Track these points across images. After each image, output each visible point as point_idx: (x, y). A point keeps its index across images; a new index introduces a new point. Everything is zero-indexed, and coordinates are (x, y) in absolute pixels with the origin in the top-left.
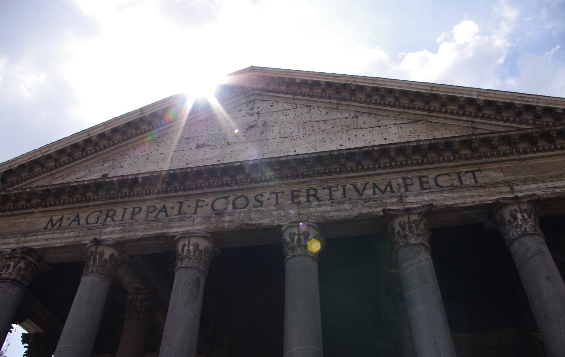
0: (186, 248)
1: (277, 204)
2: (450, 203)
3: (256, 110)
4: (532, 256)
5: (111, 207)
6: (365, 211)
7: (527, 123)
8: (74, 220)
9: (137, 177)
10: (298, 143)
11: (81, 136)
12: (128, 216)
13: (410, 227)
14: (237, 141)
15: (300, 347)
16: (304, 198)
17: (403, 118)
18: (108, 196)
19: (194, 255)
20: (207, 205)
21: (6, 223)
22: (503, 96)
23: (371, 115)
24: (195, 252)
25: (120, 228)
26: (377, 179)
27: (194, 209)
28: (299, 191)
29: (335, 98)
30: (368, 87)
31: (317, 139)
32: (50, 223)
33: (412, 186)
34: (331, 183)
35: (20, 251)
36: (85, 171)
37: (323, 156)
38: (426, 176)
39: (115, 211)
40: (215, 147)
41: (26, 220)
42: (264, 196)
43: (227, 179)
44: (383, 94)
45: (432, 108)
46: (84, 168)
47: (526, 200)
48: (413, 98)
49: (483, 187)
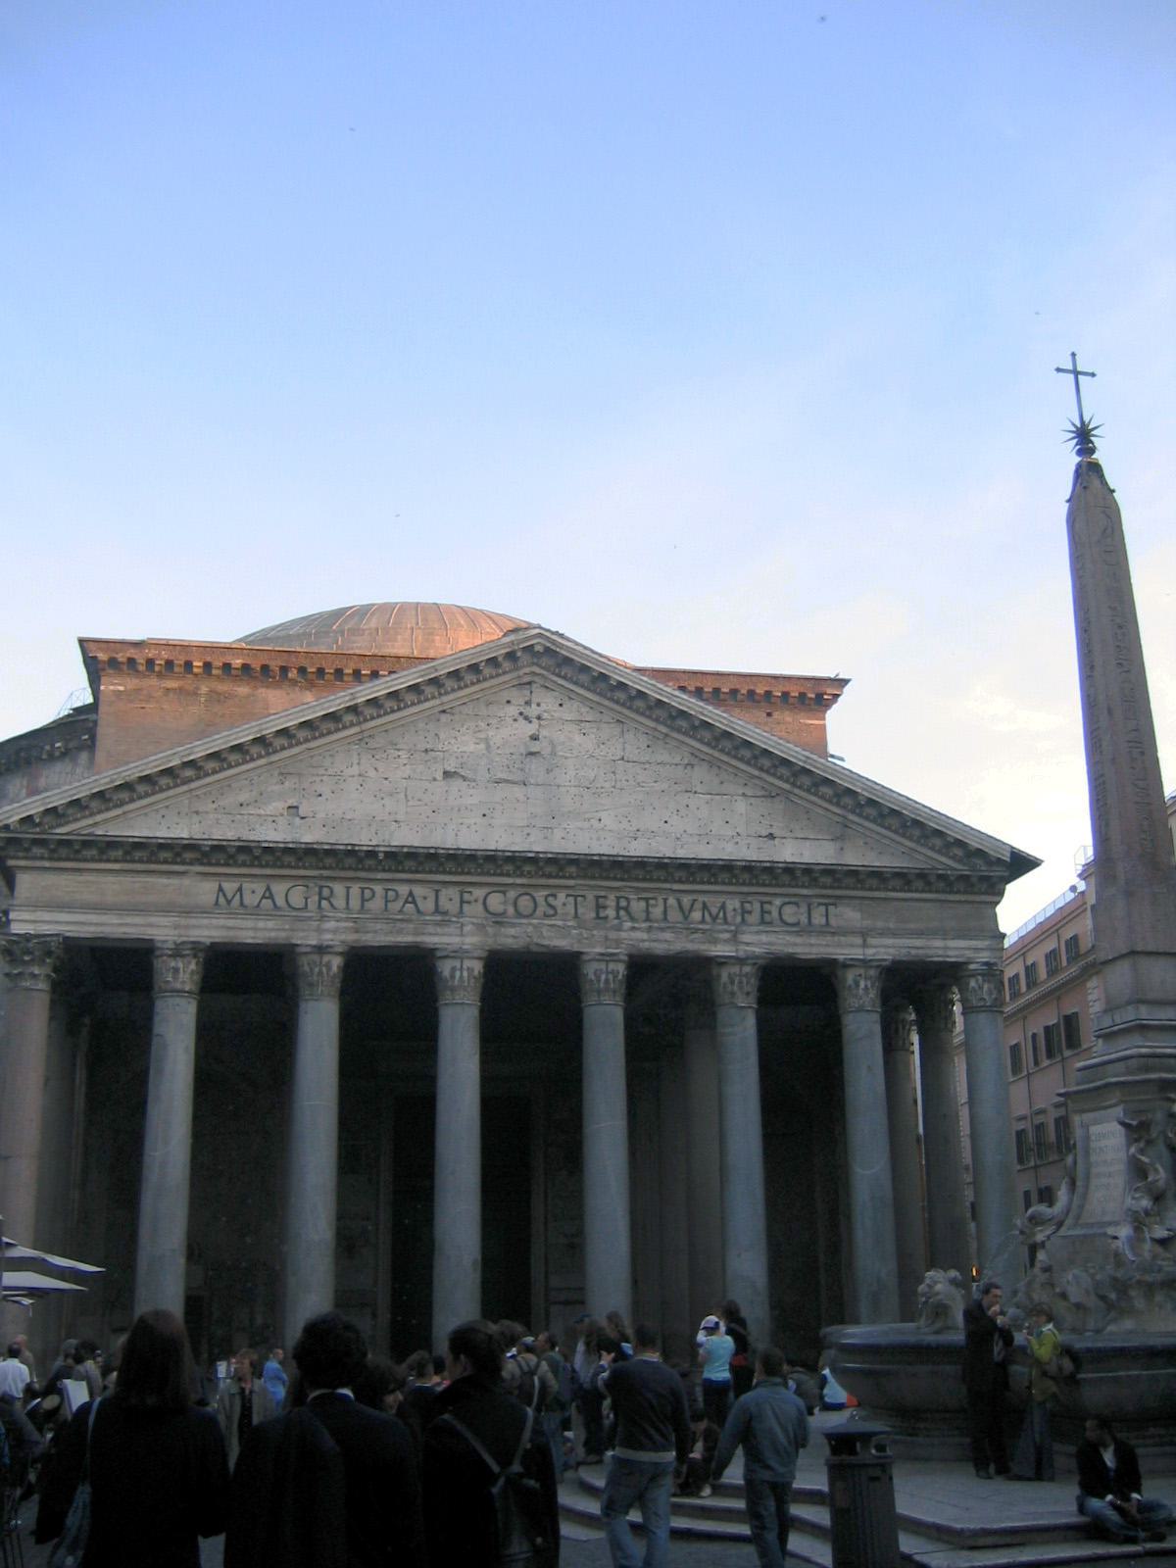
0: (458, 974)
1: (576, 915)
2: (790, 951)
3: (533, 711)
7: (910, 838)
8: (264, 897)
9: (377, 849)
11: (247, 732)
12: (355, 903)
13: (740, 982)
19: (469, 983)
20: (476, 901)
21: (134, 882)
22: (892, 800)
25: (351, 924)
27: (459, 905)
28: (605, 897)
31: (633, 801)
35: (189, 946)
39: (332, 892)
40: (474, 784)
41: (171, 881)
43: (509, 868)
45: (799, 783)
46: (247, 782)
48: (777, 763)
49: (833, 934)
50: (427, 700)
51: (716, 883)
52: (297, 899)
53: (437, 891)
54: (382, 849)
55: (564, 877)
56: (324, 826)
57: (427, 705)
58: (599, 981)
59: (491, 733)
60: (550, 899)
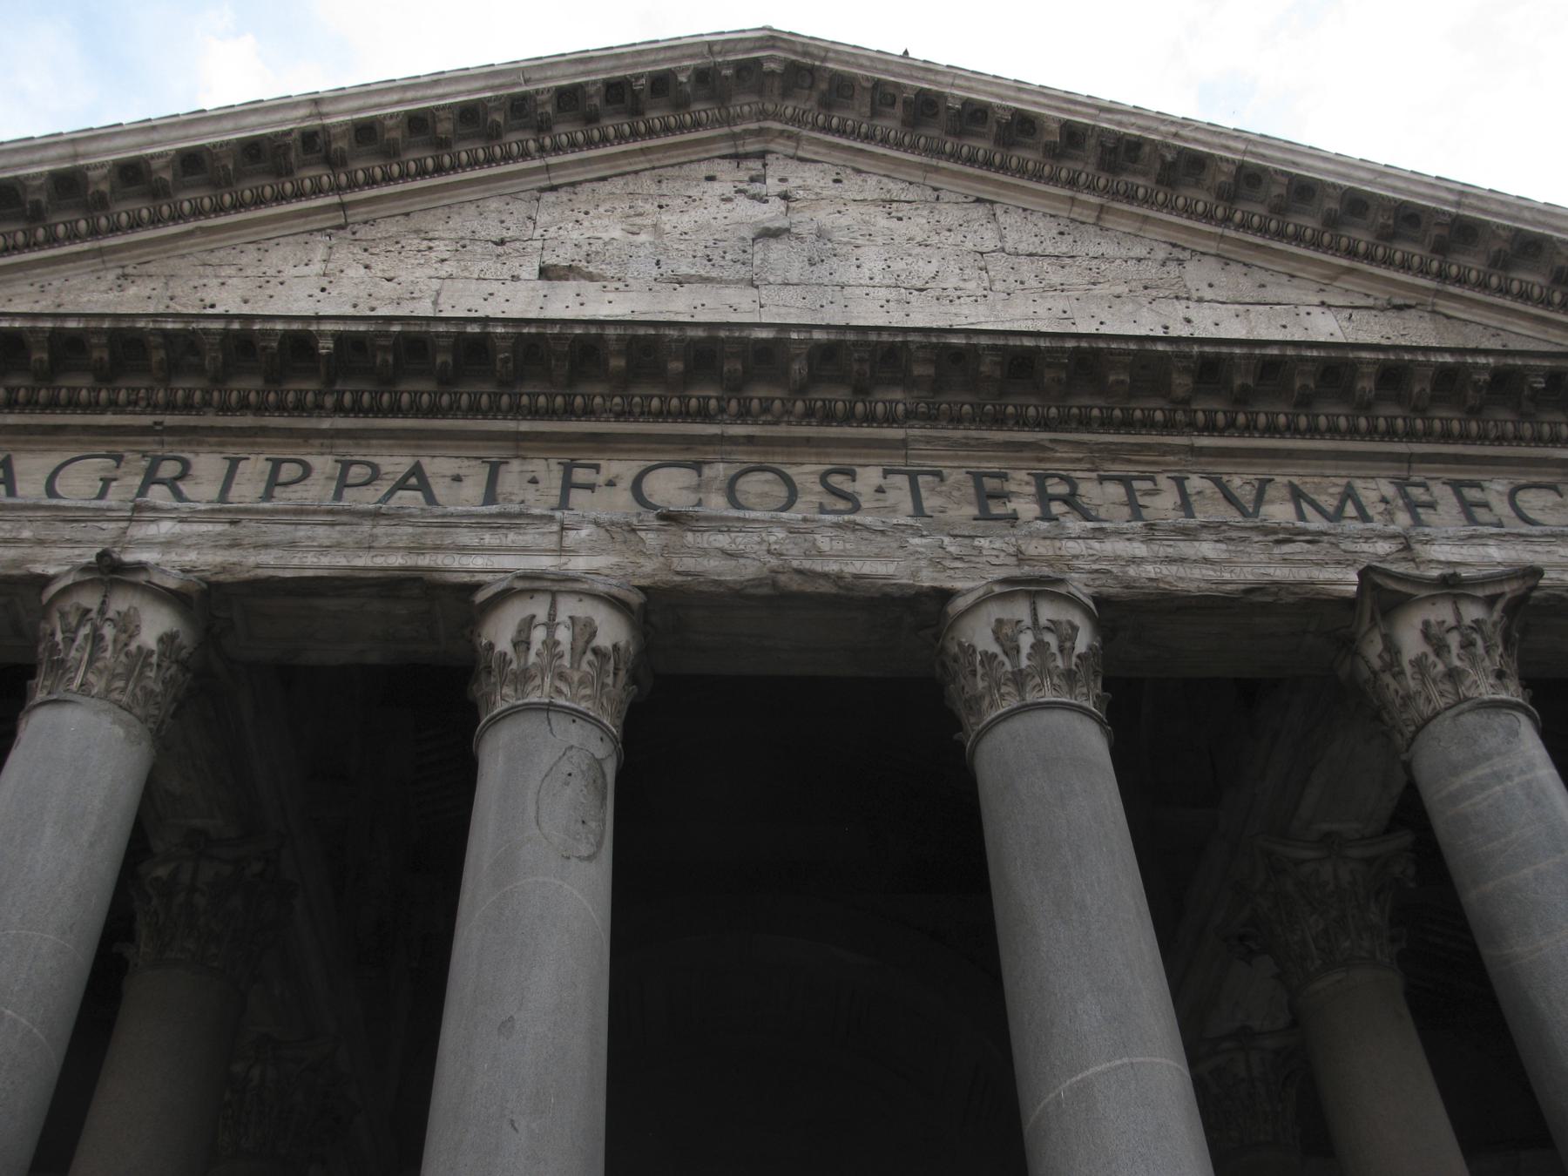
0: (538, 635)
1: (919, 511)
5: (167, 448)
6: (1278, 572)
9: (313, 328)
10: (967, 312)
12: (247, 490)
13: (1467, 645)
14: (714, 275)
15: (1126, 1060)
16: (1027, 503)
17: (1347, 290)
18: (161, 394)
20: (611, 484)
23: (1227, 264)
24: (577, 653)
25: (219, 528)
26: (1301, 471)
27: (558, 492)
29: (1091, 188)
30: (1227, 160)
33: (1435, 510)
34: (1129, 461)
36: (37, 302)
37: (1111, 352)
39: (186, 465)
40: (620, 285)
42: (858, 477)
44: (1279, 196)
45: (1454, 270)
50: (507, 158)
54: (328, 327)
55: (870, 419)
58: (1012, 650)
60: (836, 480)
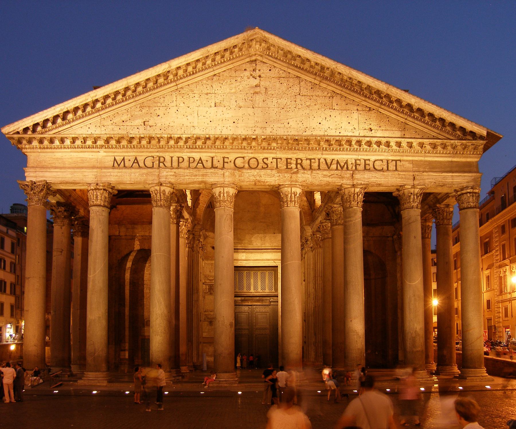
0: (222, 195)
2: (378, 182)
3: (258, 73)
4: (412, 222)
7: (437, 128)
8: (134, 162)
12: (175, 164)
20: (230, 162)
27: (222, 164)
28: (291, 159)
31: (304, 114)
32: (115, 162)
35: (101, 185)
38: (369, 160)
40: (229, 108)
46: (125, 111)
47: (419, 187)
51: (343, 150)
52: (149, 163)
53: (212, 158)
55: (271, 149)
56: (161, 130)
57: (207, 71)
58: (287, 198)
59: (238, 84)
